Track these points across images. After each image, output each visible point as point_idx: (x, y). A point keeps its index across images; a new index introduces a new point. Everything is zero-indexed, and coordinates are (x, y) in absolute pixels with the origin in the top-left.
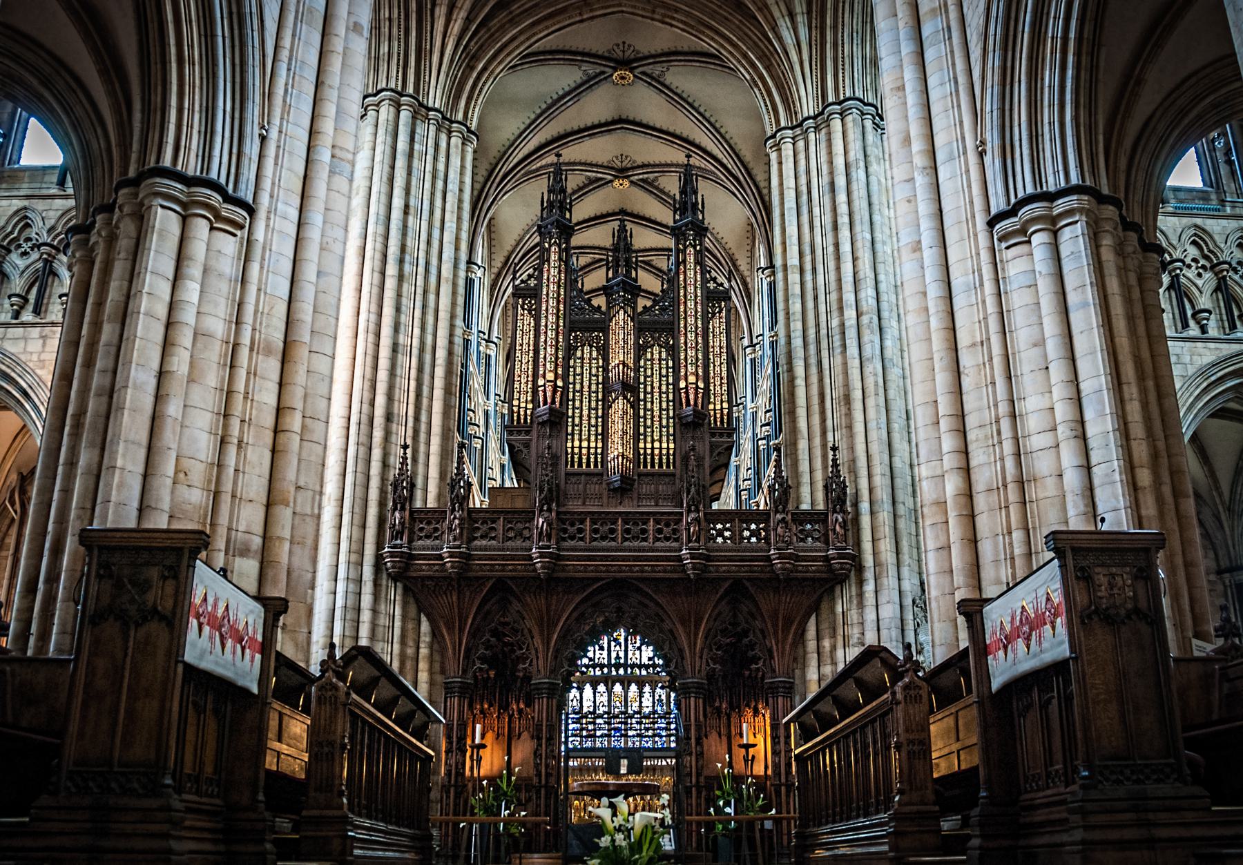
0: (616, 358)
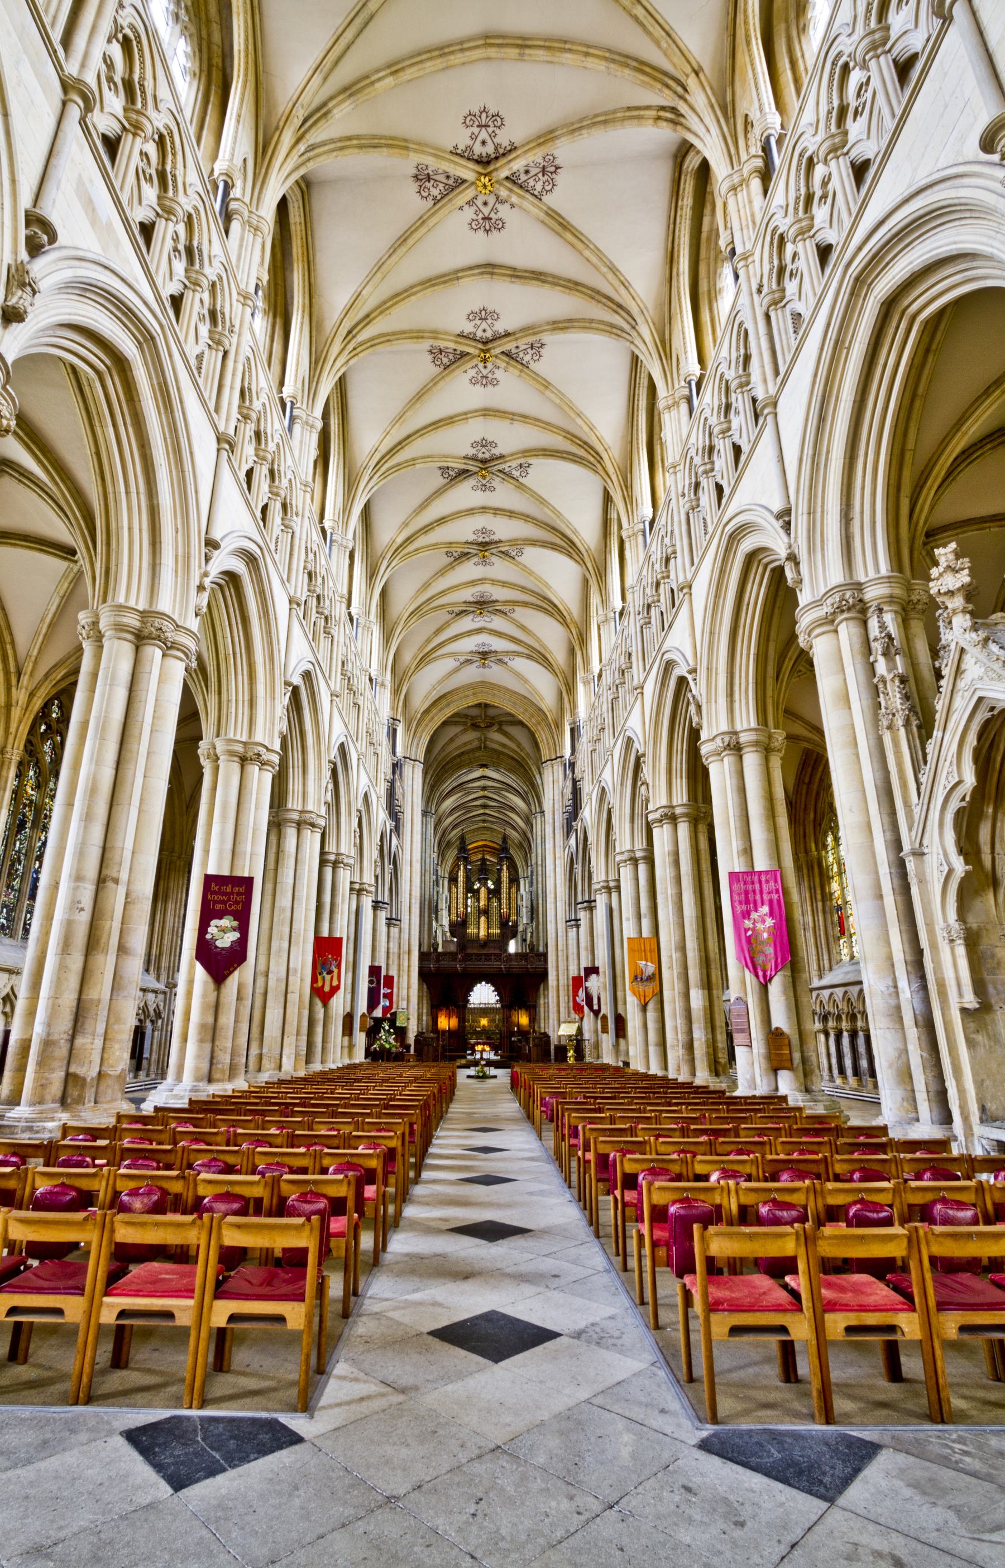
0: (483, 903)
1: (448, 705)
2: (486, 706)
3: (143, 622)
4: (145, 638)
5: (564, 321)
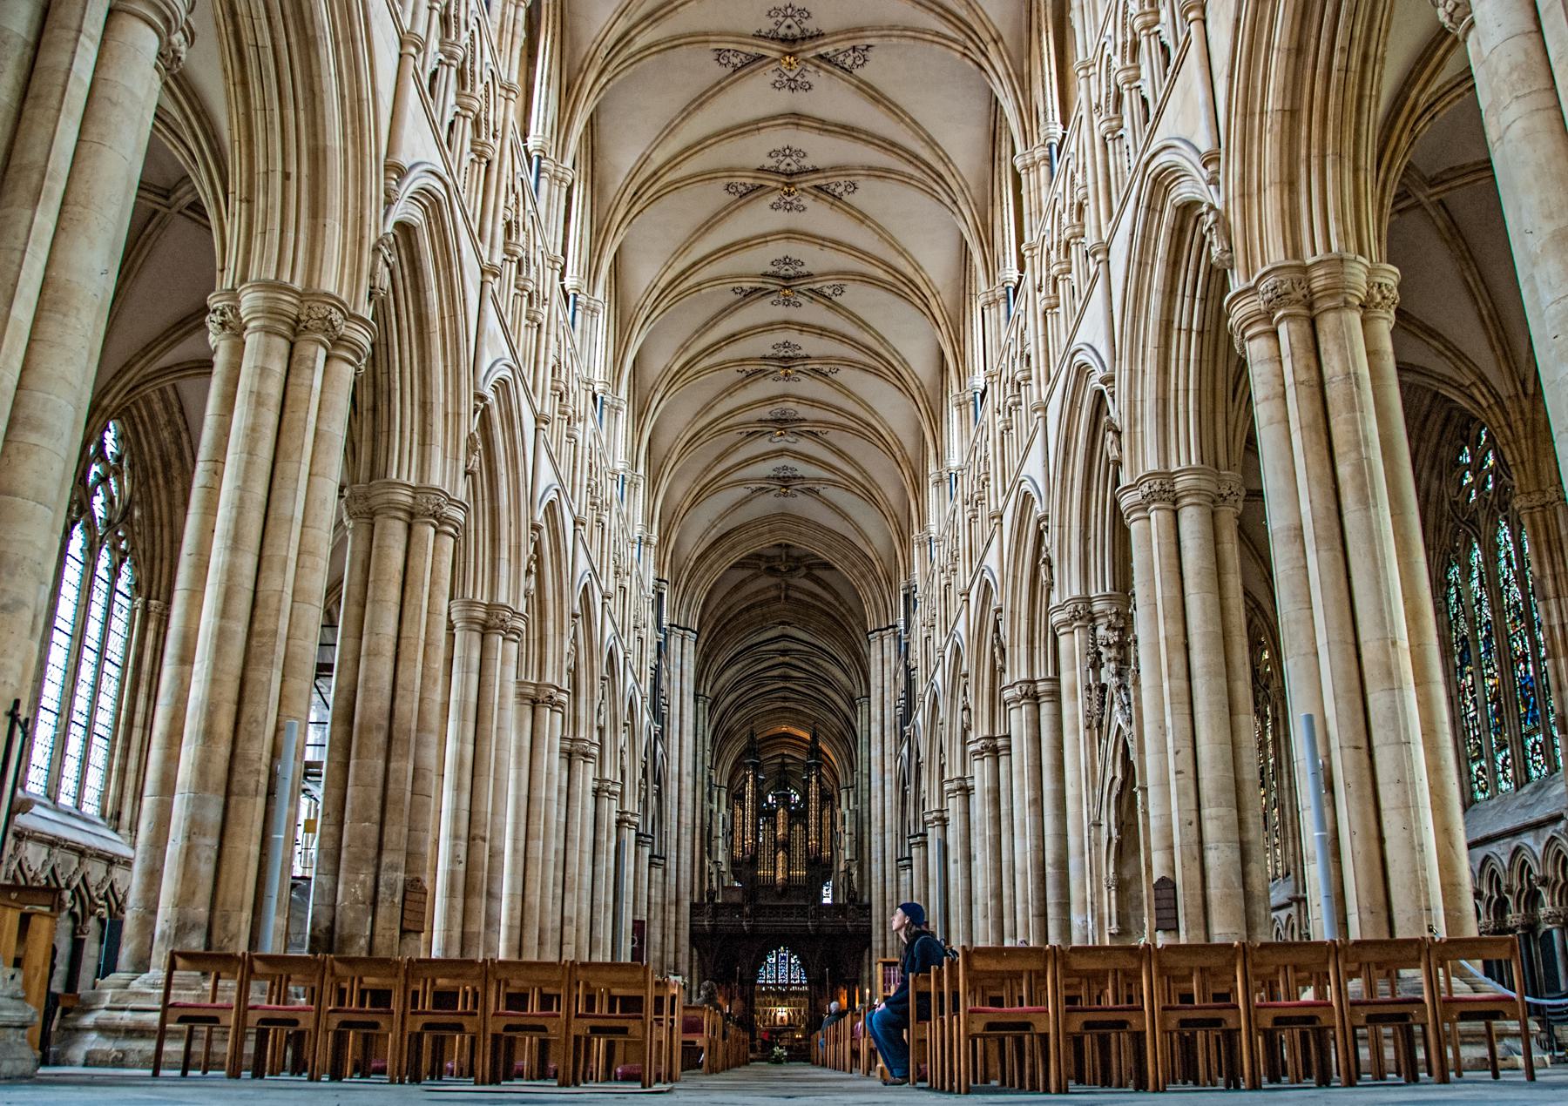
1: (733, 547)
2: (788, 546)
3: (487, 613)
4: (489, 628)
5: (880, 169)
